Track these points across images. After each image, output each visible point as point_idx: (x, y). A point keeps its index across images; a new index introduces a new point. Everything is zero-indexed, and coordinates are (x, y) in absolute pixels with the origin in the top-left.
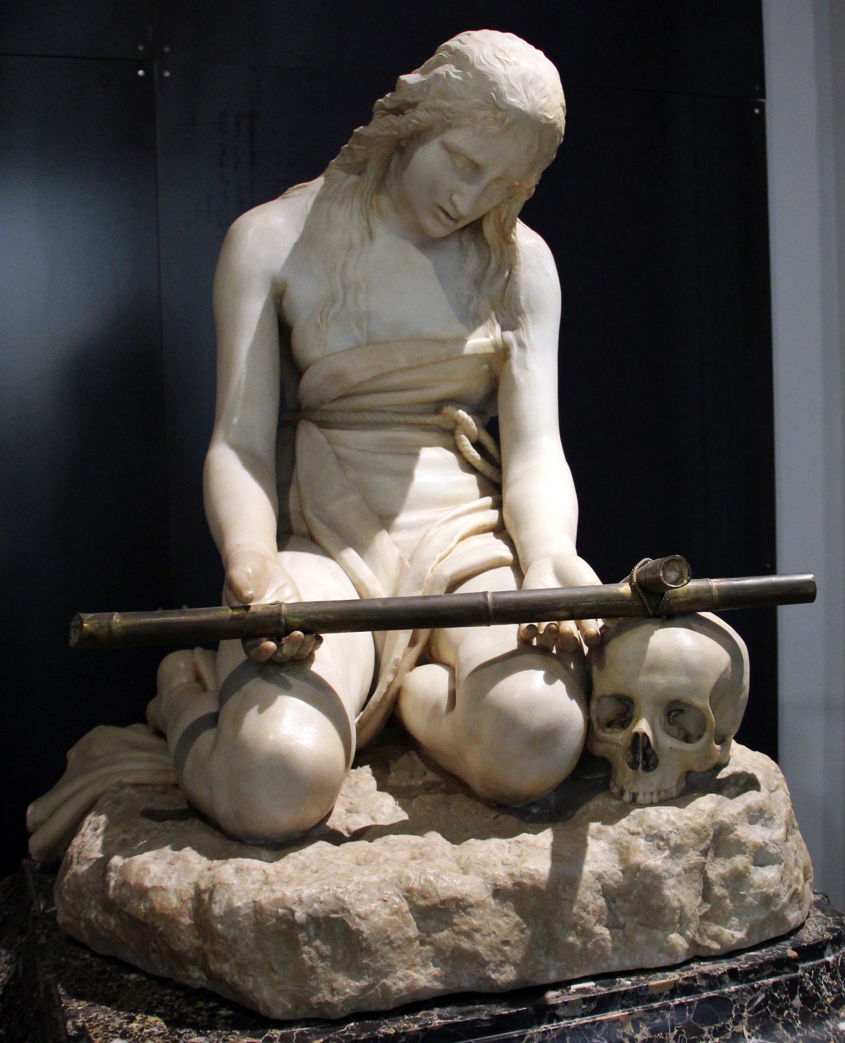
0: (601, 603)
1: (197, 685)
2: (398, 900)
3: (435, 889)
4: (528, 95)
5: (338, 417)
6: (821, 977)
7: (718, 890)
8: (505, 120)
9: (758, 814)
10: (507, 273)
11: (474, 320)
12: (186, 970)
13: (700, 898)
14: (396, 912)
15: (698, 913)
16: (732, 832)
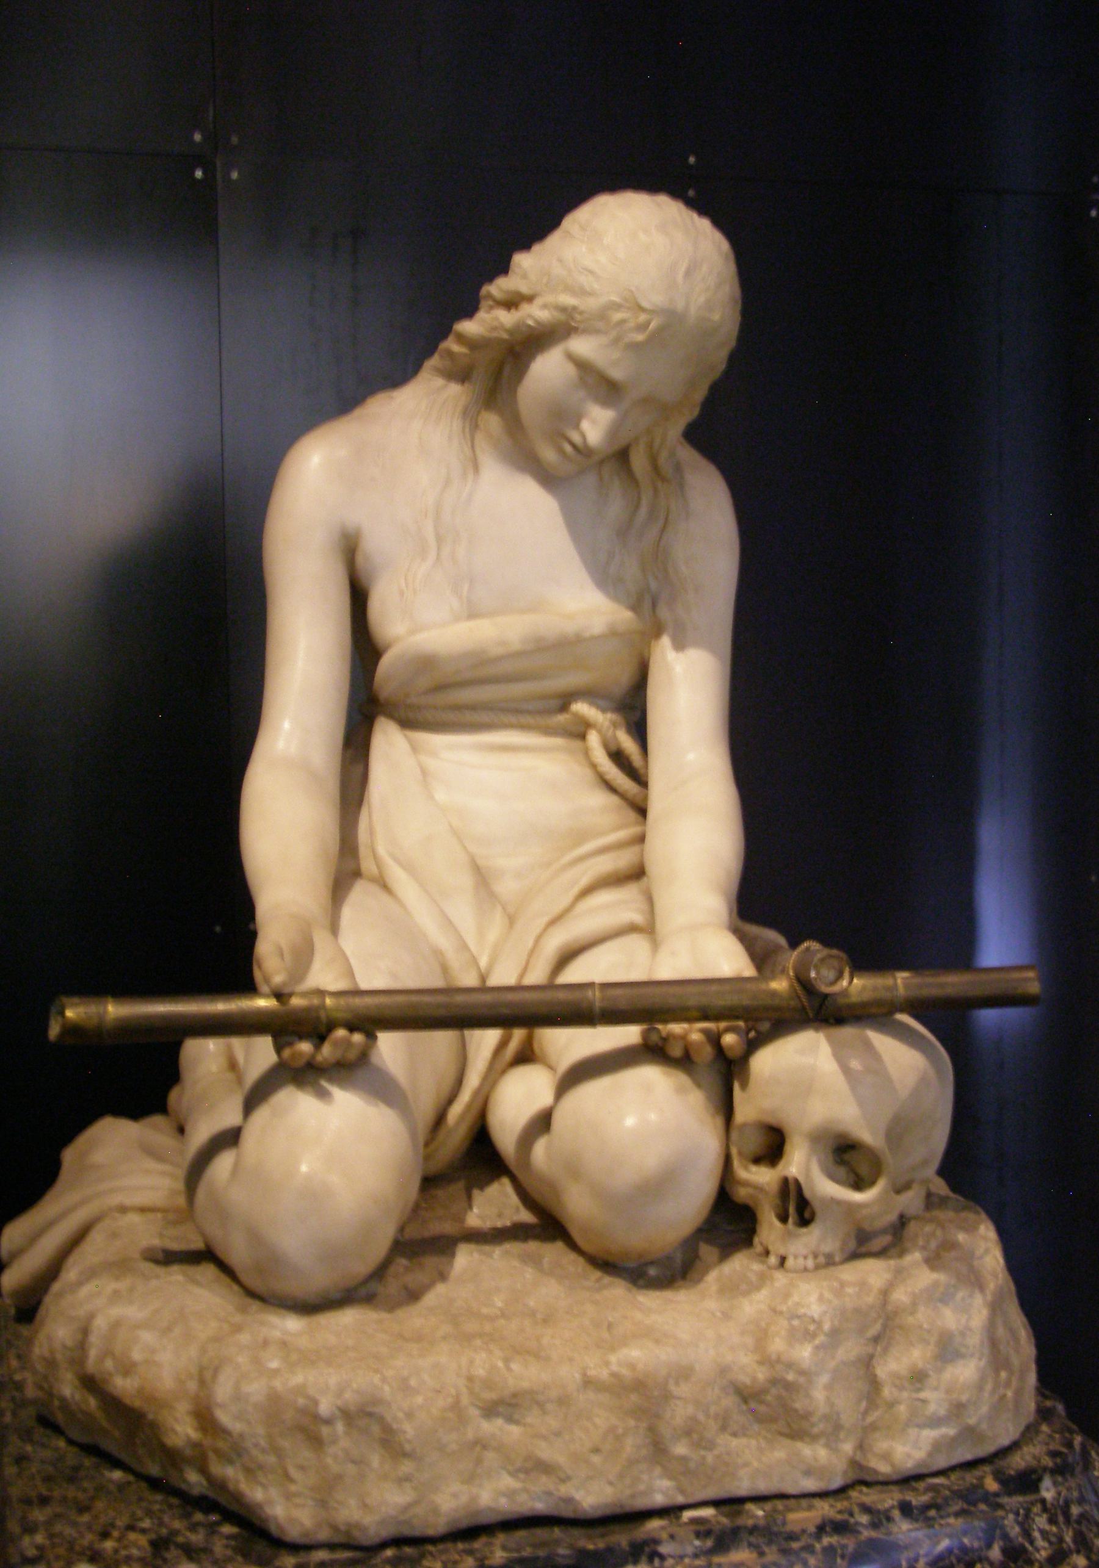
1: (230, 1076)
6: (1033, 1520)
12: (181, 1471)
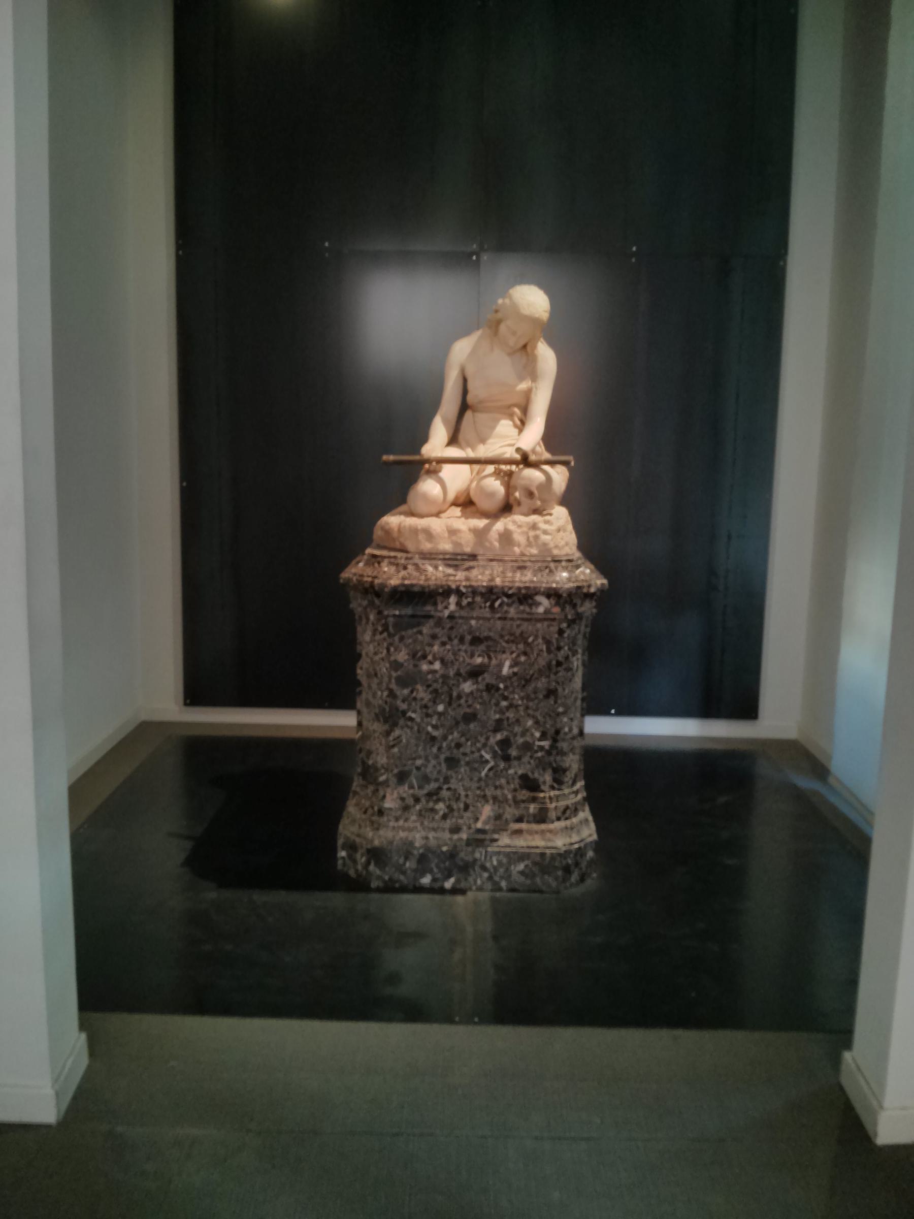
11: (521, 379)
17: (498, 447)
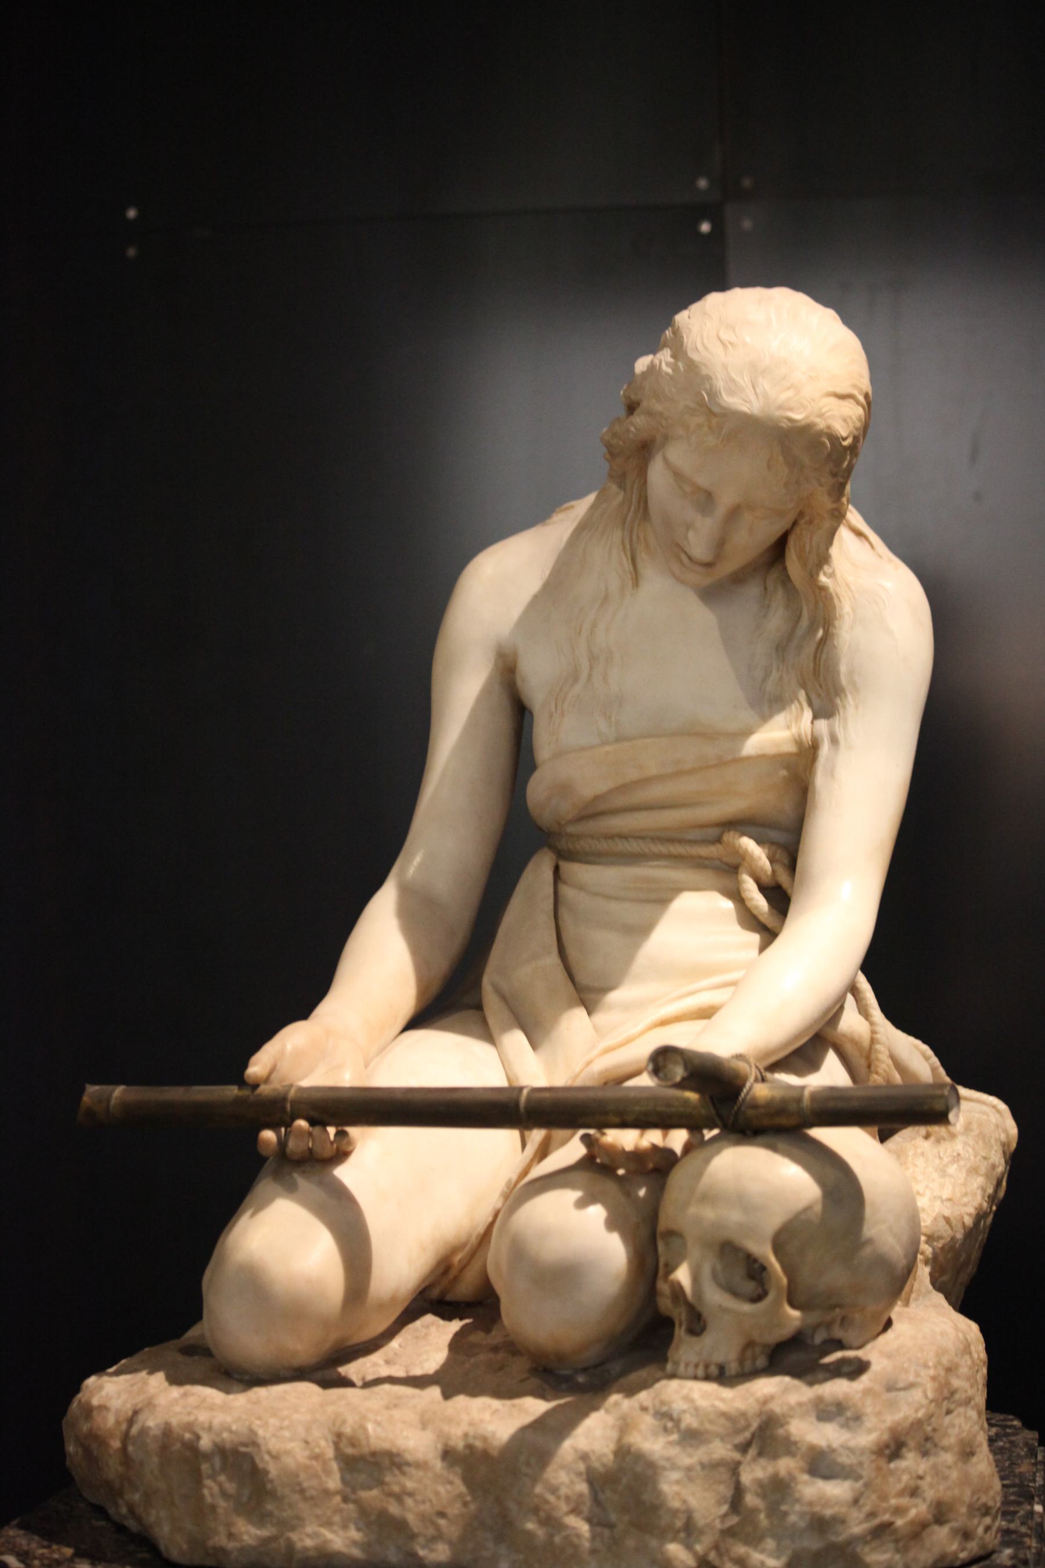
0: (658, 1109)
2: (323, 1443)
3: (367, 1437)
4: (758, 390)
5: (585, 845)
7: (751, 1500)
8: (722, 429)
9: (833, 1409)
10: (820, 633)
13: (725, 1508)
14: (316, 1457)
15: (718, 1525)
16: (782, 1426)
17: (641, 1027)
